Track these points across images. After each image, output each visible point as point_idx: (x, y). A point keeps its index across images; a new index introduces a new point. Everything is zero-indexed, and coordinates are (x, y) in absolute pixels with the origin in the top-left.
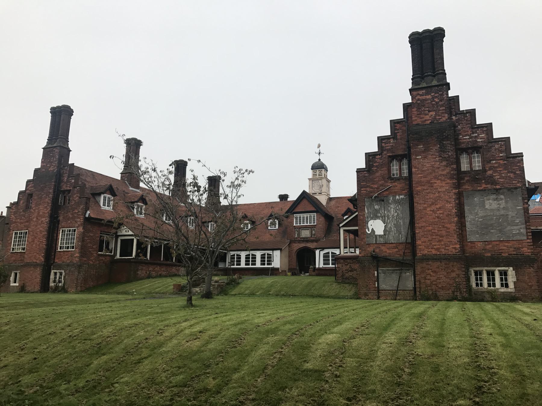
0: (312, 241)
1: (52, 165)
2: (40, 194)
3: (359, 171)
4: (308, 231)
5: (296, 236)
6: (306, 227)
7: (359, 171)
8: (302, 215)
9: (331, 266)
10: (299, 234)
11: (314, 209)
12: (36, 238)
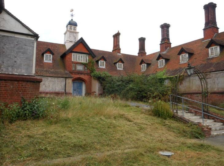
0: (85, 74)
3: (38, 35)
4: (82, 66)
6: (81, 64)
7: (38, 35)
11: (87, 52)
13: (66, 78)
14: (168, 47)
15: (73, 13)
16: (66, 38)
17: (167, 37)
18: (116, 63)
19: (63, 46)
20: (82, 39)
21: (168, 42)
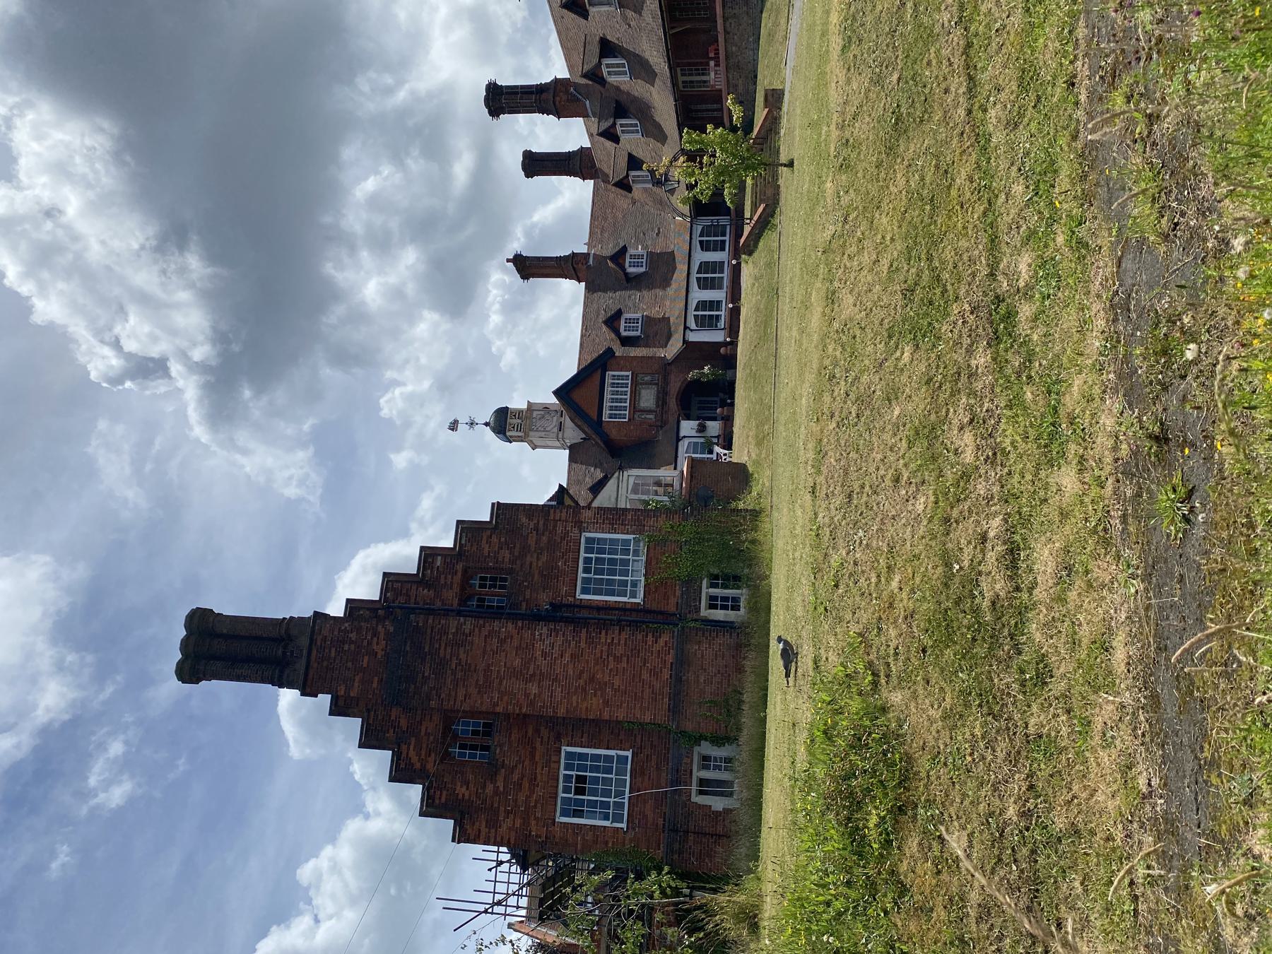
1: (369, 643)
2: (454, 673)
5: (652, 416)
8: (607, 404)
9: (727, 238)
10: (650, 412)
11: (598, 376)
12: (592, 679)
13: (678, 439)
14: (567, 92)
15: (463, 419)
16: (550, 443)
17: (532, 93)
18: (626, 274)
19: (573, 449)
20: (556, 393)
21: (552, 91)
